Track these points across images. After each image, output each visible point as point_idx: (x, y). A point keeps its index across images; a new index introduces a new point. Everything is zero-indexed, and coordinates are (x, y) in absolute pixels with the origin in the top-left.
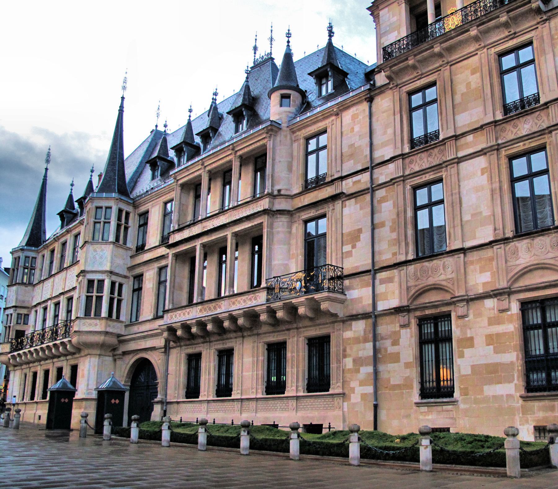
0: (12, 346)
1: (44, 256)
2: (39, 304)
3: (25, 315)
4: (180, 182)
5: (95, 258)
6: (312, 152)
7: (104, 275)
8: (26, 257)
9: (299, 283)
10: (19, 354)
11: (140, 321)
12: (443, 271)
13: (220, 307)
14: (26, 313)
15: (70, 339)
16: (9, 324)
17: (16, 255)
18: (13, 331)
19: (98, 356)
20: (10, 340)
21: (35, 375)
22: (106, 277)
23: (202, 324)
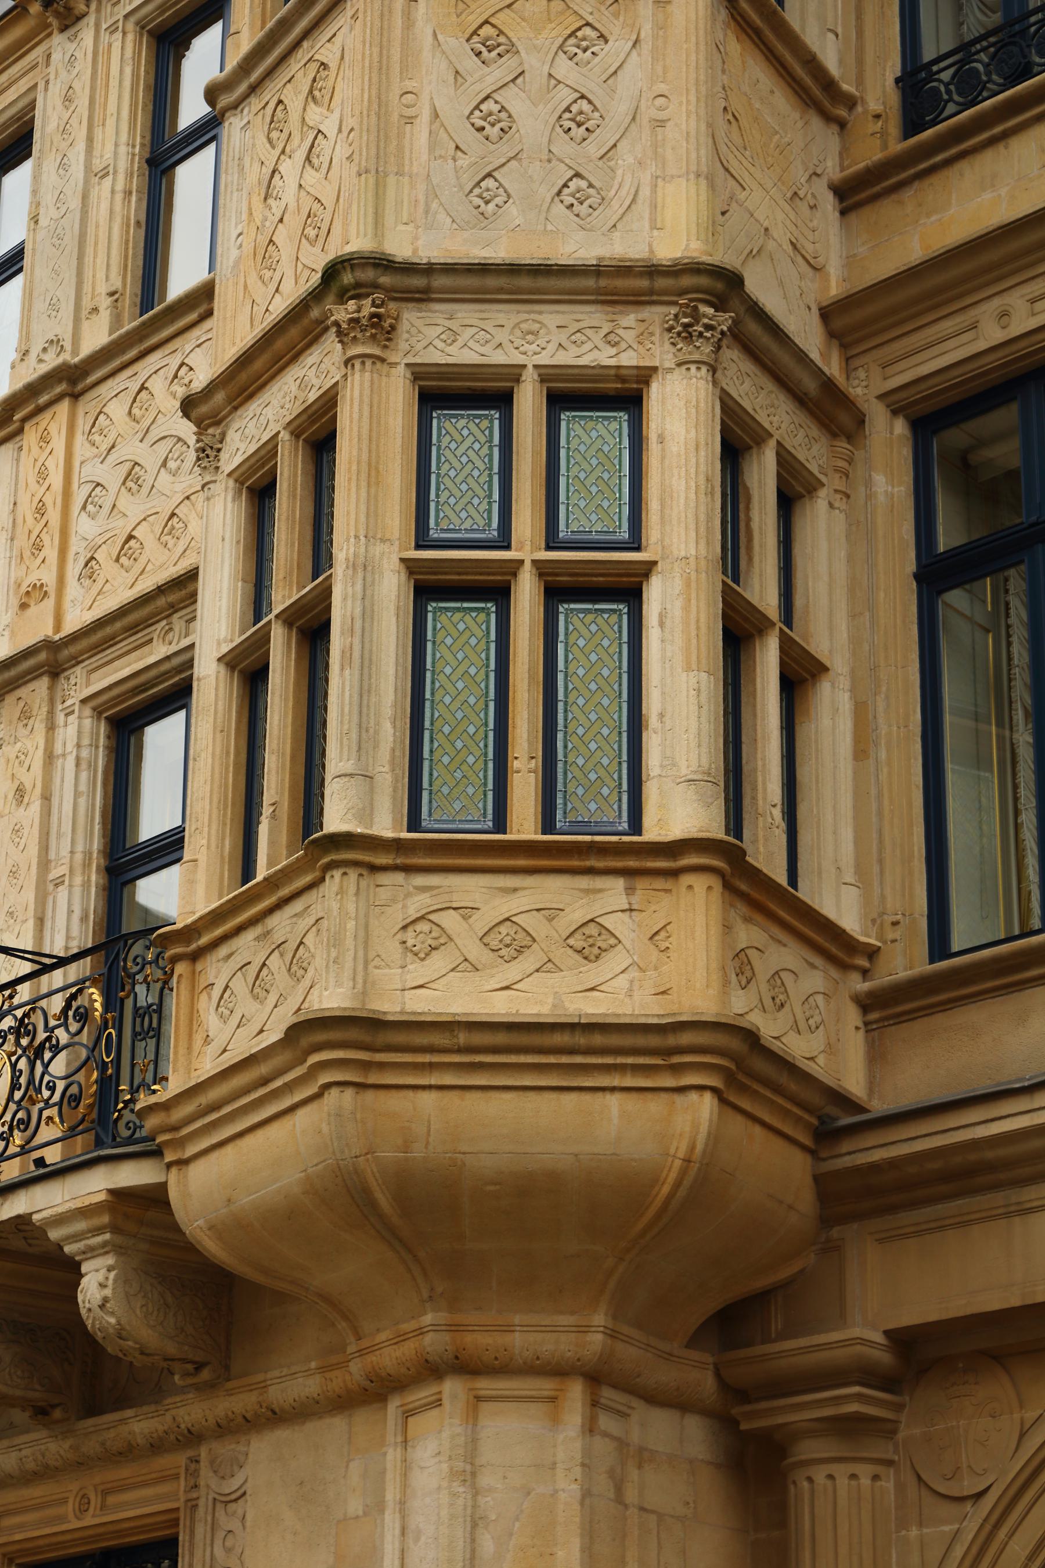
5: (491, 120)
7: (630, 319)
15: (132, 1175)
19: (576, 1391)
22: (661, 353)
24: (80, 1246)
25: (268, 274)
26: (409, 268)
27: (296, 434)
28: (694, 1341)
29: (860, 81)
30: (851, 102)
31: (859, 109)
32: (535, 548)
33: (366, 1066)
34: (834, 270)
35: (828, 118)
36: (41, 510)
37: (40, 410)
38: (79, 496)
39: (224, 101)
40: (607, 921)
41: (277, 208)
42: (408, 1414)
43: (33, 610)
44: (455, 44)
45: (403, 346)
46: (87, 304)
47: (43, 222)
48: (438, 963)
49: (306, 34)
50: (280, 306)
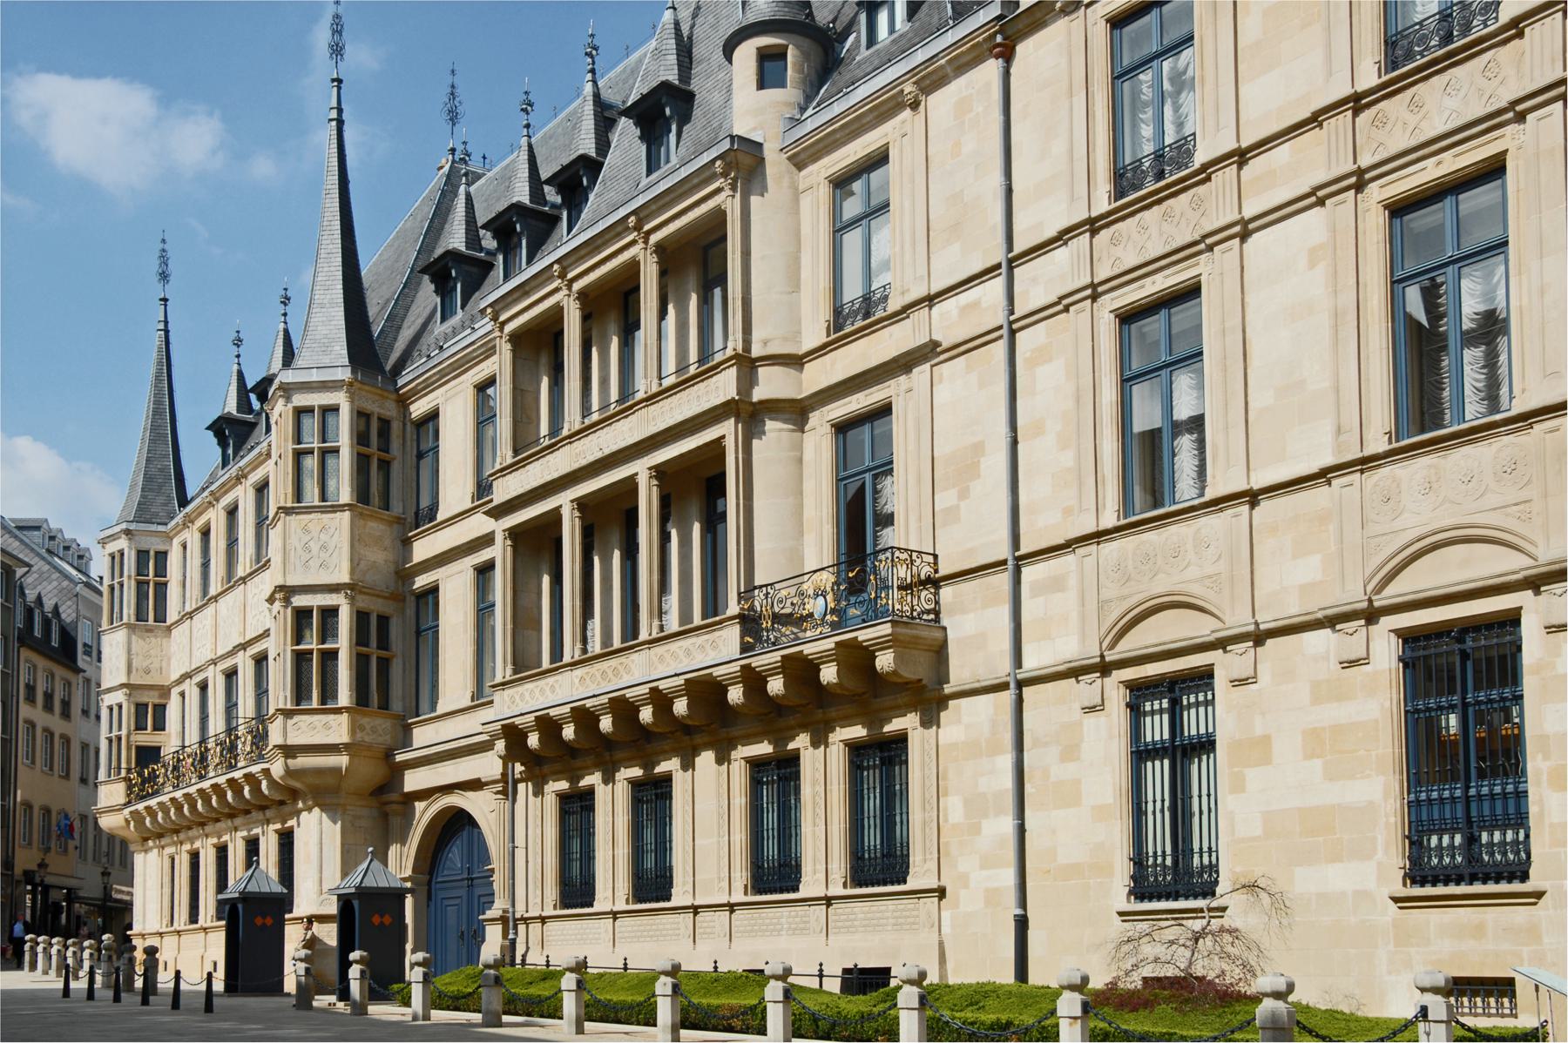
0: (130, 788)
2: (187, 676)
4: (509, 328)
6: (855, 222)
9: (821, 599)
10: (148, 808)
11: (440, 711)
12: (1186, 554)
13: (628, 670)
14: (157, 701)
18: (129, 748)
23: (585, 717)
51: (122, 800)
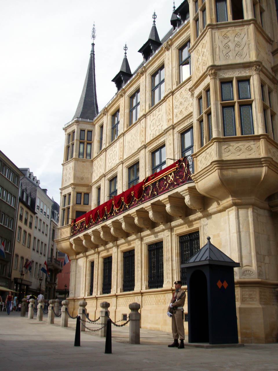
1: (102, 127)
3: (85, 194)
5: (227, 46)
8: (81, 130)
16: (66, 206)
17: (70, 130)
18: (73, 212)
20: (70, 223)
21: (108, 261)
24: (185, 194)
25: (198, 71)
26: (218, 66)
27: (204, 90)
28: (265, 200)
29: (274, 38)
30: (273, 41)
31: (274, 42)
32: (237, 100)
33: (222, 166)
34: (272, 63)
35: (270, 44)
36: (170, 109)
37: (168, 97)
38: (174, 107)
39: (190, 52)
40: (251, 146)
41: (199, 63)
42: (228, 211)
43: (170, 122)
44: (221, 37)
45: (218, 76)
46: (173, 83)
47: (167, 75)
48: (229, 153)
49: (201, 40)
50: (201, 75)
51: (69, 235)
